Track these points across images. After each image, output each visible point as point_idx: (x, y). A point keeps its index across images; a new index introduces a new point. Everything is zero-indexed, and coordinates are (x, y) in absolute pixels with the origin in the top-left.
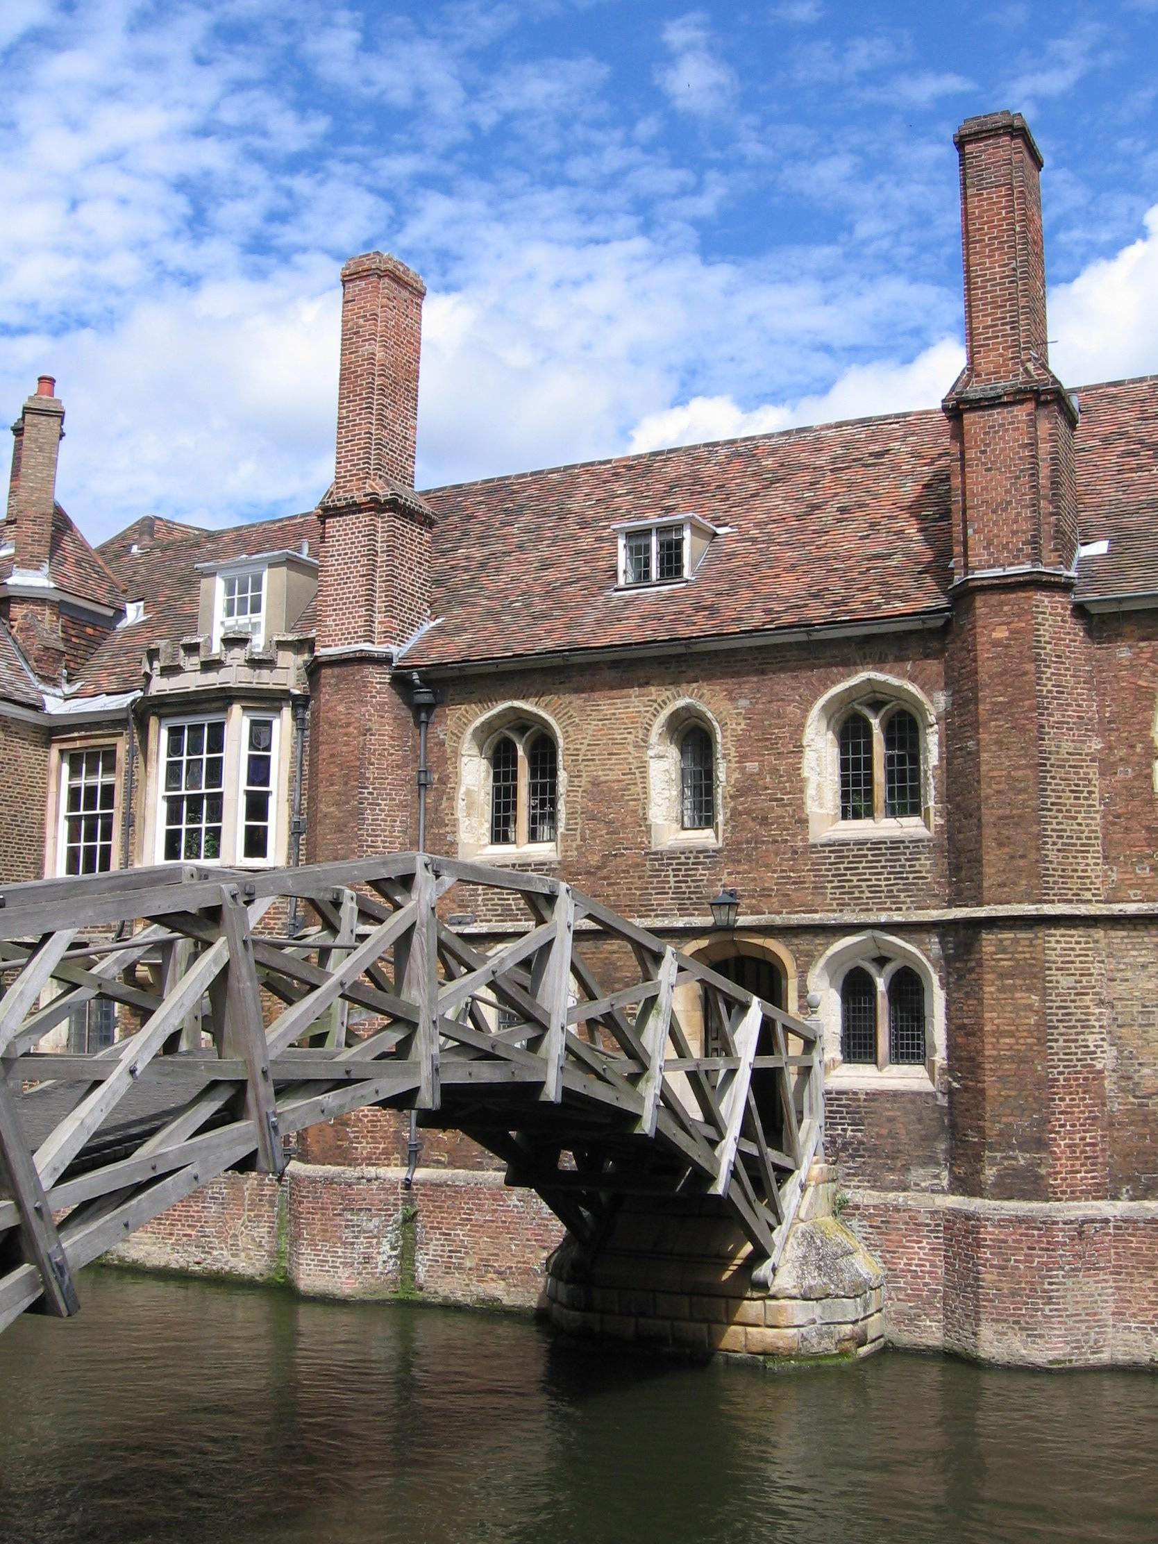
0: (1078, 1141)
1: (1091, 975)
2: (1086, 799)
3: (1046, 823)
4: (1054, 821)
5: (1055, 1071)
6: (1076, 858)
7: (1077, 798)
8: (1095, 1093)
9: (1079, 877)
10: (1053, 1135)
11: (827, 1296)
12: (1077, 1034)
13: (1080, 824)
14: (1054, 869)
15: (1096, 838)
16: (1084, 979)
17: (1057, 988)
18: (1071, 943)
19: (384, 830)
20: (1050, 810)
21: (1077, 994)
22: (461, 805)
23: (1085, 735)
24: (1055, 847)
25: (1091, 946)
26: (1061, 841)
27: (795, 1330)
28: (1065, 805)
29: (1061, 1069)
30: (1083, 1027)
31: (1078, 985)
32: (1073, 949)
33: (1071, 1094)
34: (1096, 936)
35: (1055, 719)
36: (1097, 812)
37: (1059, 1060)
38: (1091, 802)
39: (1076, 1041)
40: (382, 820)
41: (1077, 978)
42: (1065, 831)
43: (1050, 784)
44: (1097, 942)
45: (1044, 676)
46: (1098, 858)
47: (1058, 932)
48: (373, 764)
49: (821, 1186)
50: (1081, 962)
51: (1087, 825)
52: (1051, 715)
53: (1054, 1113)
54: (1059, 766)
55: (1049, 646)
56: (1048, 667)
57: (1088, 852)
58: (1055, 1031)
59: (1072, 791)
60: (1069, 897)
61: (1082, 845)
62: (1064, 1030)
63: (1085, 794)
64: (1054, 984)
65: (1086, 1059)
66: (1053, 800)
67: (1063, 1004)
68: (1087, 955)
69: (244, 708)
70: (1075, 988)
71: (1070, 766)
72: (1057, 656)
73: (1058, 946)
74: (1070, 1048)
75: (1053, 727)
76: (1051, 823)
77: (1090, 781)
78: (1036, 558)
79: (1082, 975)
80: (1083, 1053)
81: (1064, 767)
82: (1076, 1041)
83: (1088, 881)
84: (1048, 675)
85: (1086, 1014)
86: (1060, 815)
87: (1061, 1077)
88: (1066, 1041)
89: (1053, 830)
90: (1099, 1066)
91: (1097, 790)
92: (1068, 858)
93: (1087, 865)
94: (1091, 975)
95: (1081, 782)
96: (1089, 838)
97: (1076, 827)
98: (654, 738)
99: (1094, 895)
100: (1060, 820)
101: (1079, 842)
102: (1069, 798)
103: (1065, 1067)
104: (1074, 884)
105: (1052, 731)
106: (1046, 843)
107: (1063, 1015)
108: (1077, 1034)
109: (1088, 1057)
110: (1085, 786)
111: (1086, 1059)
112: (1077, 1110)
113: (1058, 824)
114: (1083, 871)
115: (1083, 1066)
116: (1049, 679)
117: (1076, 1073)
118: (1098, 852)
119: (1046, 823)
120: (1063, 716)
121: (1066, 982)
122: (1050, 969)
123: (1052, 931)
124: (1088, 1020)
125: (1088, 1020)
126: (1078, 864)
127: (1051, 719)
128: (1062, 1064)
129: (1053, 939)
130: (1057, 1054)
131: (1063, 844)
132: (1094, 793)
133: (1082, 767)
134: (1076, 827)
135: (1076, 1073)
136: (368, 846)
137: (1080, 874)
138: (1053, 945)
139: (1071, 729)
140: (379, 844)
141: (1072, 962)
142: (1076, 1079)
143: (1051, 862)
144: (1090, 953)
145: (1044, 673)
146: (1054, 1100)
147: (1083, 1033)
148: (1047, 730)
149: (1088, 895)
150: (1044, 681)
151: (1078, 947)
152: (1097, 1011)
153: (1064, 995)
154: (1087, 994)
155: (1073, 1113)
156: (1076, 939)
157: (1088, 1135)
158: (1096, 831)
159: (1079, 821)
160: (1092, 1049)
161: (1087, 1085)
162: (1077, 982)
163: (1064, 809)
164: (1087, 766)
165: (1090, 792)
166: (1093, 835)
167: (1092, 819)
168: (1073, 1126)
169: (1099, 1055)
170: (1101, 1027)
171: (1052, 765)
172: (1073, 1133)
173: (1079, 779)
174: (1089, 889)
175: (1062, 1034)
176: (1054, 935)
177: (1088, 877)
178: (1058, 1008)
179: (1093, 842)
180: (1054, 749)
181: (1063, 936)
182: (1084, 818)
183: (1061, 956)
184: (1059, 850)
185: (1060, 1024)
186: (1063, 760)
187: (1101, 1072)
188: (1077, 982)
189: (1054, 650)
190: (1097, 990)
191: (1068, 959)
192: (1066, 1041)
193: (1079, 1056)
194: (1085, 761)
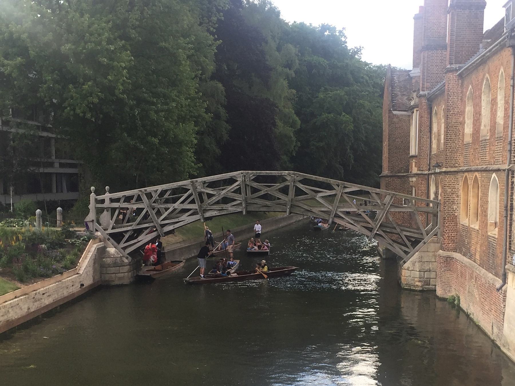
0: (450, 235)
1: (455, 188)
2: (458, 136)
3: (447, 144)
4: (449, 143)
5: (445, 215)
6: (454, 154)
7: (455, 136)
8: (455, 222)
9: (455, 160)
10: (444, 233)
11: (413, 270)
12: (451, 205)
13: (456, 144)
14: (448, 158)
15: (460, 148)
16: (454, 189)
17: (447, 192)
18: (450, 179)
19: (425, 145)
20: (448, 140)
21: (451, 194)
22: (433, 136)
23: (459, 116)
24: (449, 151)
25: (456, 180)
26: (450, 149)
27: (406, 278)
28: (452, 138)
29: (447, 215)
30: (452, 203)
31: (452, 191)
32: (451, 181)
33: (449, 222)
34: (457, 177)
35: (451, 113)
36: (461, 140)
37: (446, 212)
38: (459, 137)
39: (451, 207)
40: (425, 142)
41: (452, 189)
42: (452, 146)
43: (449, 133)
44: (457, 179)
45: (449, 100)
46: (460, 154)
47: (447, 176)
48: (422, 126)
49: (432, 244)
50: (453, 185)
51: (458, 144)
52: (451, 112)
53: (444, 227)
54: (451, 127)
55: (451, 90)
56: (451, 97)
57: (458, 152)
58: (446, 204)
59: (454, 134)
60: (452, 166)
61: (456, 150)
62: (448, 204)
63: (458, 135)
64: (446, 191)
65: (453, 212)
66: (450, 137)
67: (448, 197)
68: (454, 183)
69: (417, 111)
70: (451, 192)
71: (454, 127)
72: (453, 93)
73: (447, 180)
74: (449, 209)
75: (451, 115)
76: (448, 144)
77: (459, 130)
78: (451, 64)
79: (453, 188)
80: (452, 211)
81: (453, 127)
82: (451, 207)
83: (457, 161)
84: (450, 99)
85: (454, 200)
86: (451, 142)
87: (447, 217)
88: (448, 207)
89: (449, 146)
90: (456, 214)
91: (461, 133)
92: (452, 154)
93: (457, 156)
94: (455, 188)
95: (457, 131)
96: (458, 148)
97: (455, 145)
98: (442, 117)
99: (458, 165)
100: (451, 143)
101: (455, 149)
102: (453, 136)
103: (448, 214)
104: (453, 162)
105: (450, 116)
106: (447, 150)
107: (448, 200)
108: (451, 205)
109: (453, 212)
110: (458, 132)
111: (453, 212)
112: (450, 226)
113: (450, 144)
114: (456, 158)
115: (452, 214)
116: (450, 101)
117: (450, 216)
118: (460, 152)
119: (447, 144)
120: (453, 111)
121: (449, 190)
122: (445, 186)
123: (446, 176)
124: (454, 201)
125: (454, 201)
126: (455, 156)
127: (450, 113)
128: (447, 213)
129: (446, 178)
130: (446, 211)
131: (451, 150)
132: (460, 134)
133: (457, 126)
134: (455, 145)
135: (450, 216)
136: (422, 149)
137: (455, 159)
138: (446, 180)
139: (455, 115)
140: (424, 148)
141: (451, 185)
142: (451, 218)
143: (448, 156)
144: (455, 182)
145: (449, 99)
146: (445, 223)
147: (452, 205)
148: (449, 116)
149: (457, 165)
150: (449, 101)
151: (452, 180)
152: (457, 199)
153: (448, 194)
154: (454, 194)
155: (449, 227)
156: (452, 178)
157: (453, 234)
158: (460, 146)
159: (456, 143)
160: (455, 210)
161: (453, 220)
162: (452, 190)
163: (452, 140)
164: (459, 126)
165: (460, 134)
166: (459, 147)
167: (460, 142)
168: (449, 231)
169: (456, 211)
170: (457, 203)
171: (449, 127)
172: (449, 233)
173: (457, 130)
174: (457, 163)
175: (447, 205)
176: (447, 177)
177: (457, 160)
178: (447, 198)
179: (459, 149)
180: (450, 122)
181: (449, 177)
182: (457, 142)
183: (448, 183)
184: (450, 152)
185: (447, 202)
186: (453, 125)
187: (457, 216)
188: (452, 190)
189: (453, 91)
190: (457, 193)
191: (450, 184)
192: (448, 207)
193: (451, 211)
194: (458, 124)
